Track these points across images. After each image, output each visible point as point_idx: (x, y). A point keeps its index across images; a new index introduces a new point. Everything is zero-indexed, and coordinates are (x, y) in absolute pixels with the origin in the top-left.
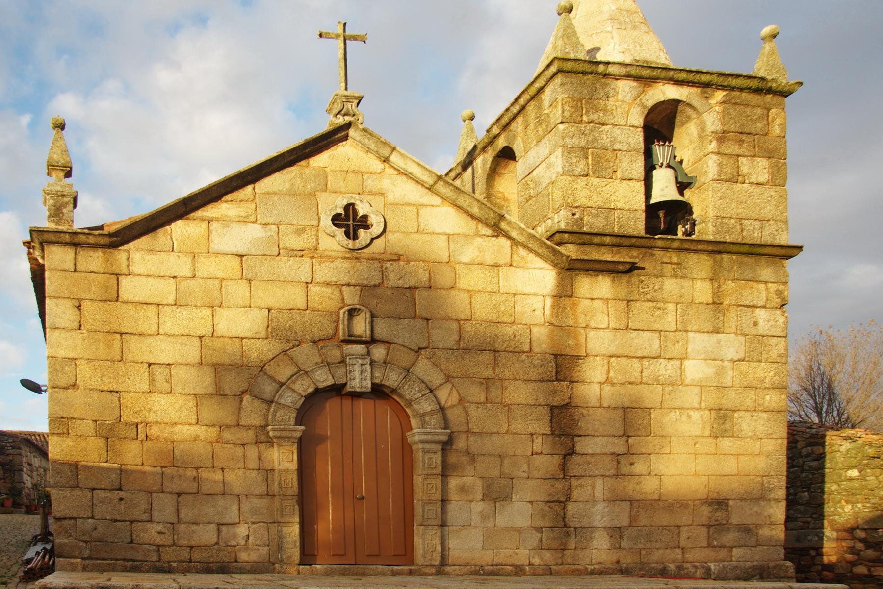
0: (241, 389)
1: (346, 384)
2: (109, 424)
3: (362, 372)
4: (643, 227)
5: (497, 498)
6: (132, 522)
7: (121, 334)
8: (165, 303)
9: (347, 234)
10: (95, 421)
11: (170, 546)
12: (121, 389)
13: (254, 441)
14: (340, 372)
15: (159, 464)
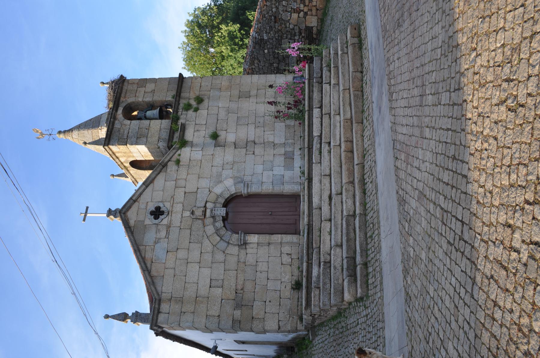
1: (223, 217)
6: (280, 298)
7: (197, 297)
9: (162, 215)
12: (221, 299)
14: (217, 218)
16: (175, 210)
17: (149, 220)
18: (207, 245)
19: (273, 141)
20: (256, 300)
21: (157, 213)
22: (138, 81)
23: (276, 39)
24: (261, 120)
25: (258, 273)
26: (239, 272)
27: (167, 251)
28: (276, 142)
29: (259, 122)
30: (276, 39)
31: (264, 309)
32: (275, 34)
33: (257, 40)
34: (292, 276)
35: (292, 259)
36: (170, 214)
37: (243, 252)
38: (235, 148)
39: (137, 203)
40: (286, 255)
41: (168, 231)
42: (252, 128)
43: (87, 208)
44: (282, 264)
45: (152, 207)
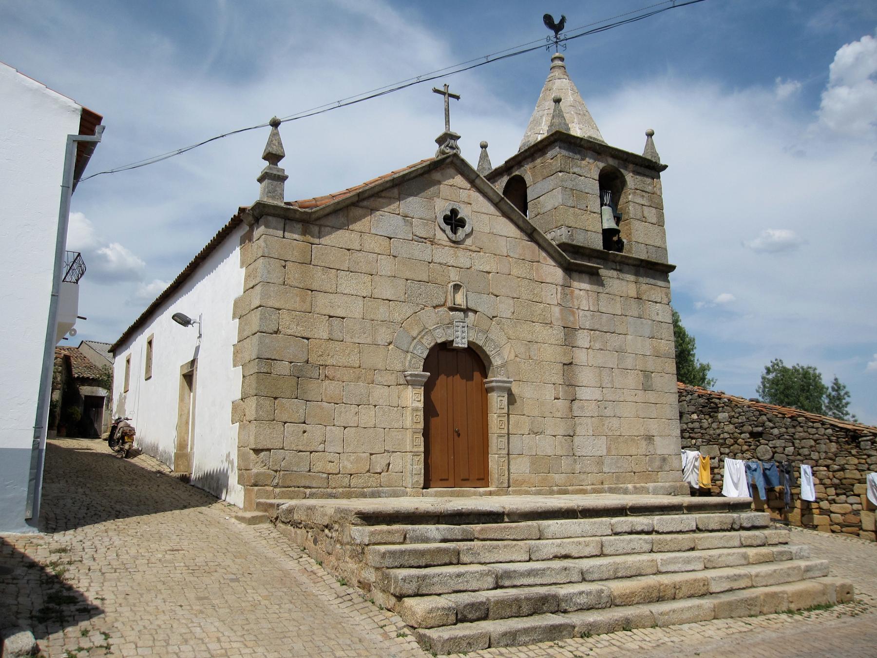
0: (388, 341)
1: (453, 341)
2: (300, 365)
3: (463, 332)
4: (602, 244)
5: (537, 433)
6: (311, 452)
8: (342, 269)
9: (452, 229)
10: (291, 363)
11: (336, 474)
12: (309, 336)
13: (395, 384)
15: (333, 401)
16: (460, 253)
17: (442, 207)
18: (401, 312)
19: (577, 433)
20: (308, 405)
21: (454, 221)
22: (658, 193)
23: (719, 435)
24: (608, 412)
25: (354, 409)
26: (357, 371)
27: (390, 238)
28: (576, 439)
29: (605, 408)
30: (719, 435)
31: (293, 420)
32: (729, 434)
33: (717, 401)
34: (351, 475)
35: (380, 473)
36: (452, 245)
37: (391, 379)
38: (564, 364)
39: (468, 186)
40: (387, 462)
41: (424, 241)
42: (597, 394)
43: (458, 98)
44: (371, 454)
45: (464, 212)
